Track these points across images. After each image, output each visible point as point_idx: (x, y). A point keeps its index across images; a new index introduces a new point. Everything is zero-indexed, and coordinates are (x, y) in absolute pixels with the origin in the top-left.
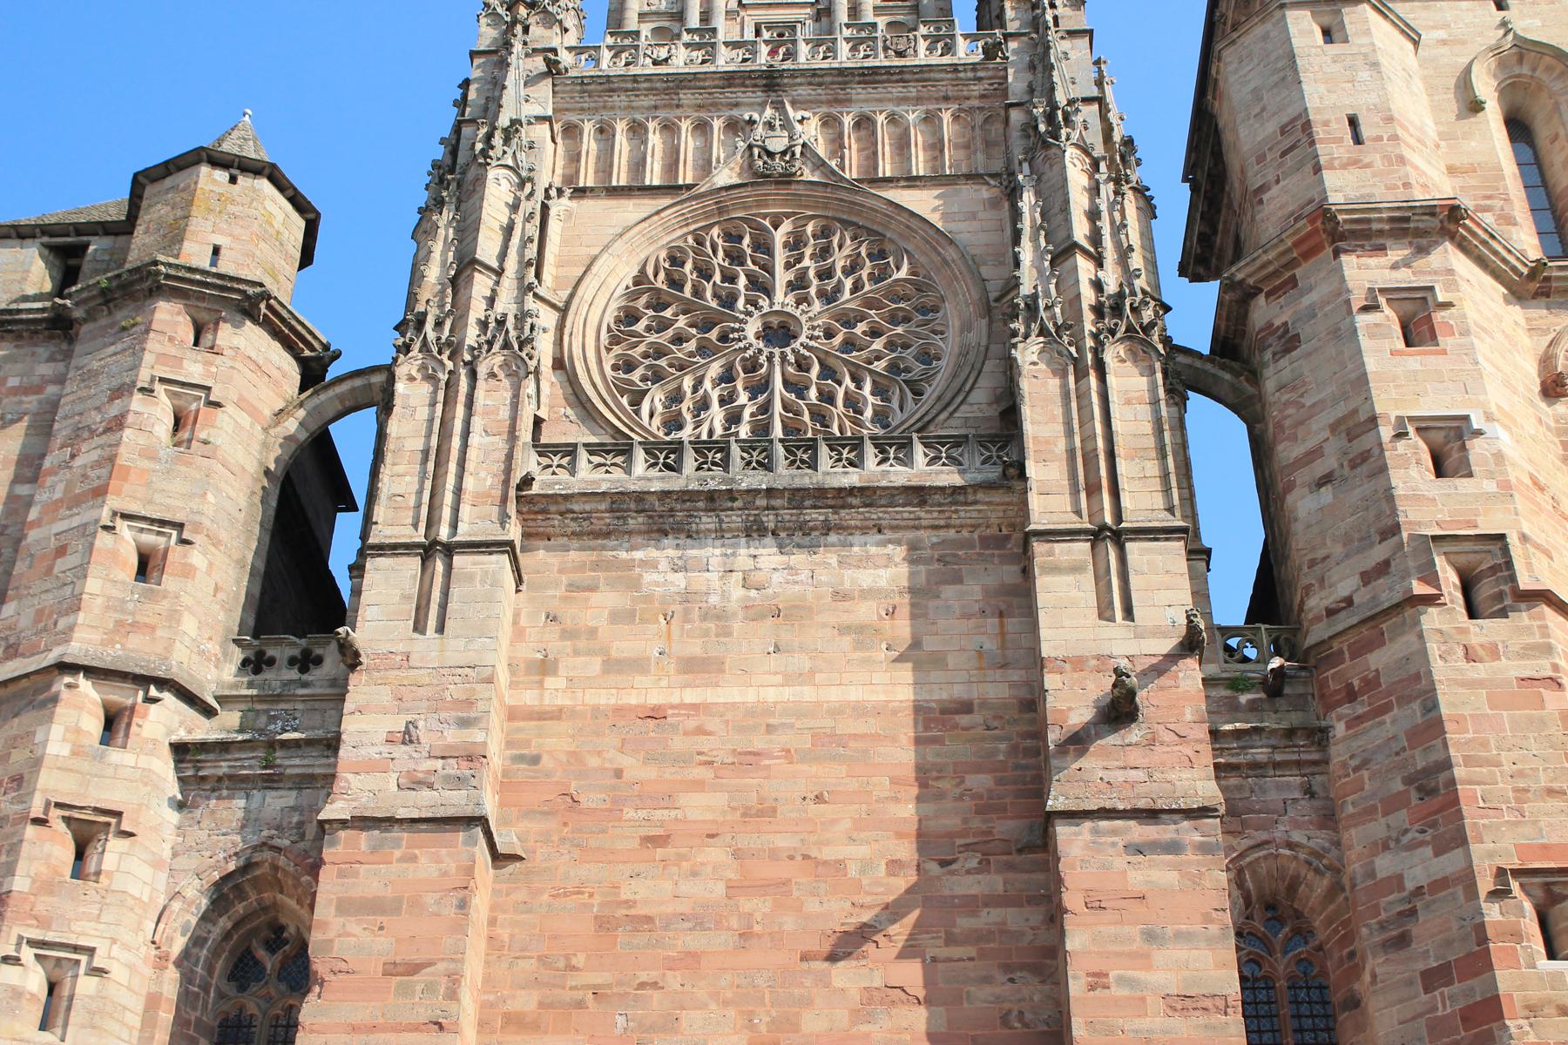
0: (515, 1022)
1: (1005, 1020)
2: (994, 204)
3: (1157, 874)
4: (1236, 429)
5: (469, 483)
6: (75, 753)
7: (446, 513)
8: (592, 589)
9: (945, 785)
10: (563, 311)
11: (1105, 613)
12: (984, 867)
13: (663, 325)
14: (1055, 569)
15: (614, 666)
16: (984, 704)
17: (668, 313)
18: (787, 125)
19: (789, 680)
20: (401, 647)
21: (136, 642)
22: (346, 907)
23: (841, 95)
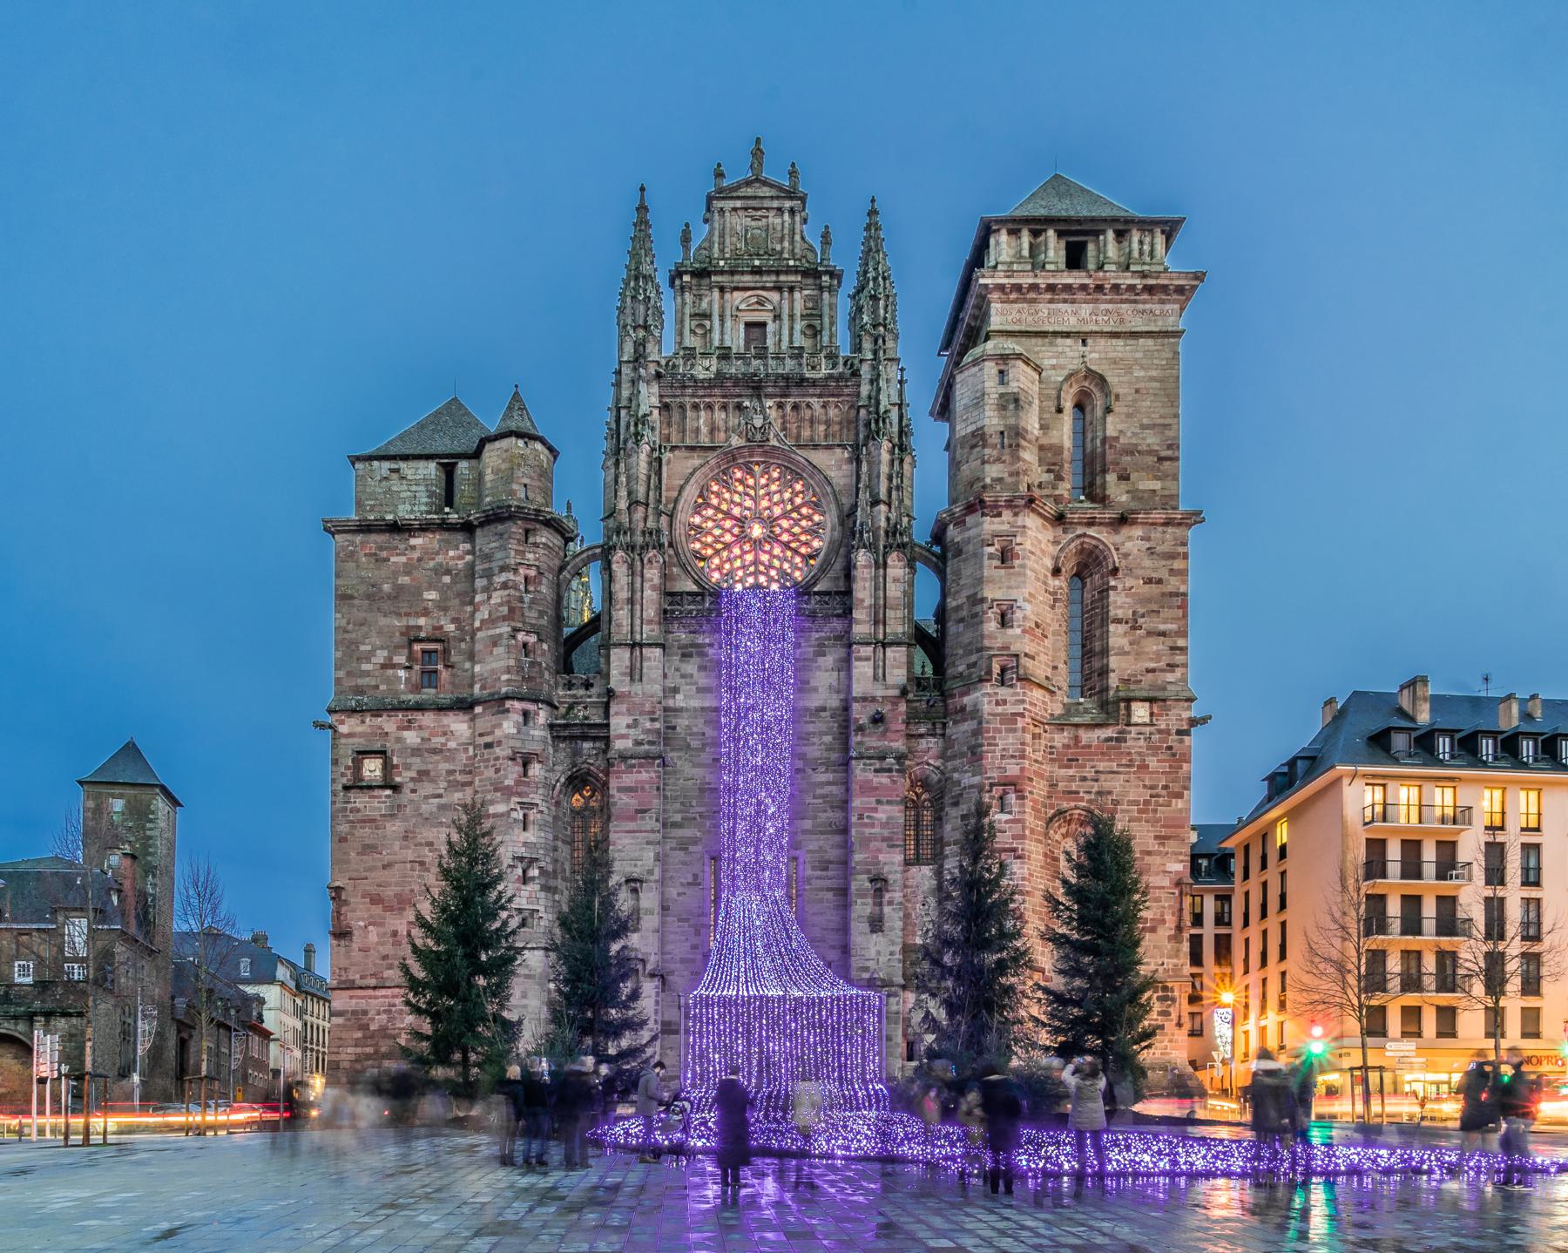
0: (675, 825)
2: (850, 461)
3: (884, 779)
6: (519, 732)
7: (637, 628)
8: (690, 655)
9: (815, 740)
10: (671, 516)
11: (875, 678)
14: (860, 659)
18: (763, 411)
20: (625, 689)
22: (620, 790)
23: (787, 392)
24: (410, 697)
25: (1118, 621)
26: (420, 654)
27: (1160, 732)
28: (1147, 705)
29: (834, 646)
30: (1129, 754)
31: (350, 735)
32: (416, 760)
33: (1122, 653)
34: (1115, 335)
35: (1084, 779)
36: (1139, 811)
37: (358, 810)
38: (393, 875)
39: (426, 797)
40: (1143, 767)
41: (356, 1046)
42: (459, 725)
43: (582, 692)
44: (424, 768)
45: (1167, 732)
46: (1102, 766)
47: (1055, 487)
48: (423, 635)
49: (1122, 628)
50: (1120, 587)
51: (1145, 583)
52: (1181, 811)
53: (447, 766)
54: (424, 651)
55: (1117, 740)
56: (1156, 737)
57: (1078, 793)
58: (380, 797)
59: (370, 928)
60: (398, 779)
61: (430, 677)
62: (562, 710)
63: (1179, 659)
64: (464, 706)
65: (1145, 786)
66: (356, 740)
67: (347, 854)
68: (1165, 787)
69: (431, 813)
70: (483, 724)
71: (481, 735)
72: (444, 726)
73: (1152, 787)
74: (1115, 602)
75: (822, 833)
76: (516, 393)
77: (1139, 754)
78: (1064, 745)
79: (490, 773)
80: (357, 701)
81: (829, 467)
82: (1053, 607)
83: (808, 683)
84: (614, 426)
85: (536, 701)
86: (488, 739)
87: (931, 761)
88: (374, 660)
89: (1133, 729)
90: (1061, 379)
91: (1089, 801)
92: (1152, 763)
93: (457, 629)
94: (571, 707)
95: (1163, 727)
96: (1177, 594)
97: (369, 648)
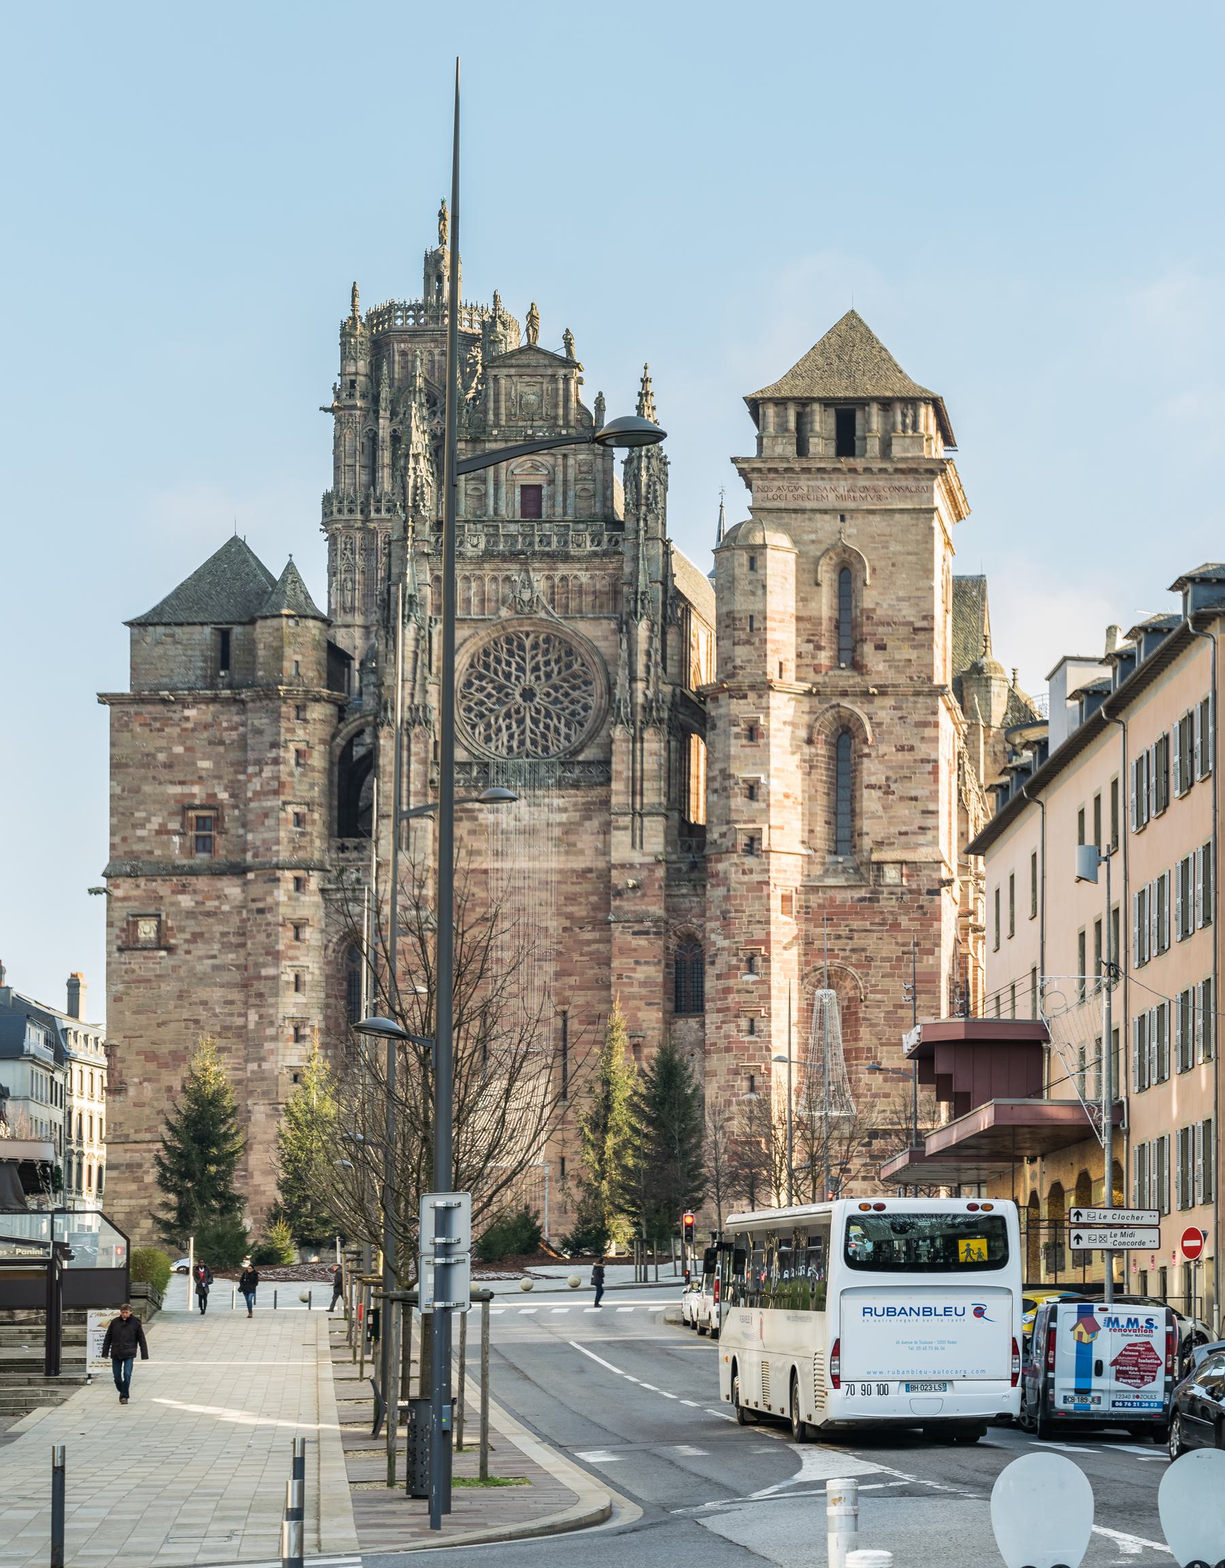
1: (597, 981)
4: (702, 747)
5: (412, 788)
9: (582, 900)
12: (593, 930)
13: (482, 689)
15: (471, 853)
16: (597, 869)
17: (484, 683)
19: (532, 858)
21: (301, 854)
24: (185, 862)
25: (870, 787)
26: (194, 821)
27: (911, 891)
28: (898, 866)
29: (600, 810)
30: (882, 913)
31: (125, 899)
32: (192, 922)
33: (874, 816)
34: (871, 512)
35: (839, 937)
36: (892, 967)
37: (133, 971)
38: (168, 1033)
39: (200, 958)
40: (896, 926)
41: (131, 1198)
42: (232, 889)
43: (355, 855)
44: (198, 930)
45: (918, 892)
46: (856, 925)
47: (814, 657)
48: (197, 802)
49: (876, 794)
50: (873, 754)
51: (898, 750)
52: (932, 965)
53: (218, 929)
54: (198, 818)
55: (870, 899)
56: (907, 897)
57: (832, 950)
58: (154, 958)
59: (145, 1084)
60: (173, 941)
61: (204, 844)
62: (335, 873)
63: (929, 822)
64: (238, 870)
65: (897, 943)
66: (130, 904)
67: (122, 1012)
68: (917, 944)
69: (205, 974)
70: (256, 890)
71: (253, 900)
72: (218, 890)
73: (904, 945)
74: (869, 769)
75: (588, 989)
76: (290, 564)
77: (892, 913)
78: (819, 906)
79: (262, 937)
80: (132, 866)
81: (597, 638)
82: (809, 774)
83: (575, 845)
84: (386, 596)
85: (308, 869)
86: (260, 905)
87: (694, 920)
88: (148, 826)
89: (885, 890)
90: (819, 554)
91: (843, 958)
92: (904, 922)
93: (231, 796)
94: (342, 871)
95: (914, 887)
96: (928, 761)
97: (143, 814)
